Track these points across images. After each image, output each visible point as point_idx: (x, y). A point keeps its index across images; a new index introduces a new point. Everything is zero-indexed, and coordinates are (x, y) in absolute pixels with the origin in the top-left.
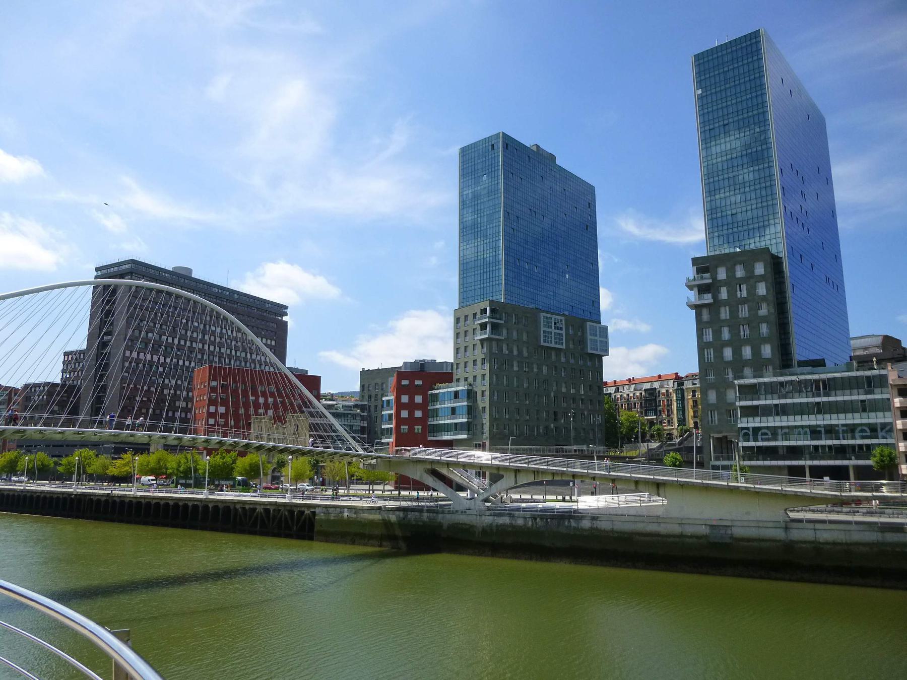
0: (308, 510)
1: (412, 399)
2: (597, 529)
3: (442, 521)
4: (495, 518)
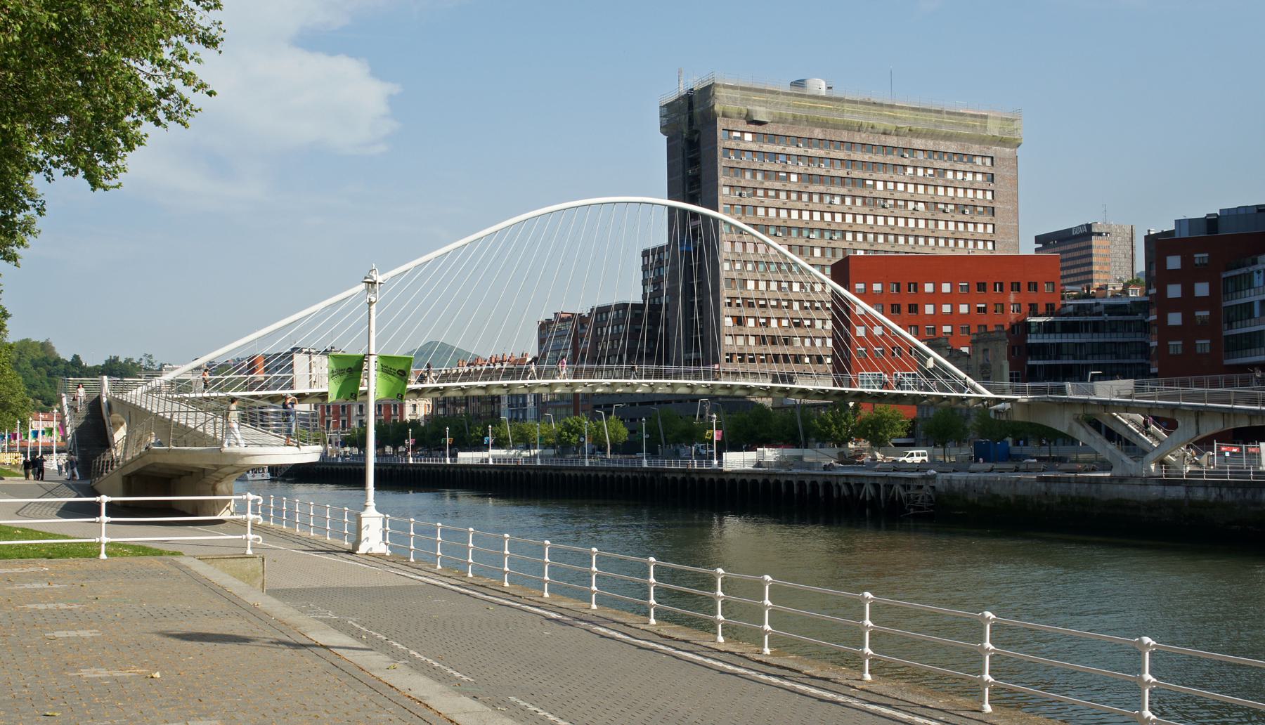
1: (1188, 290)
4: (1166, 488)
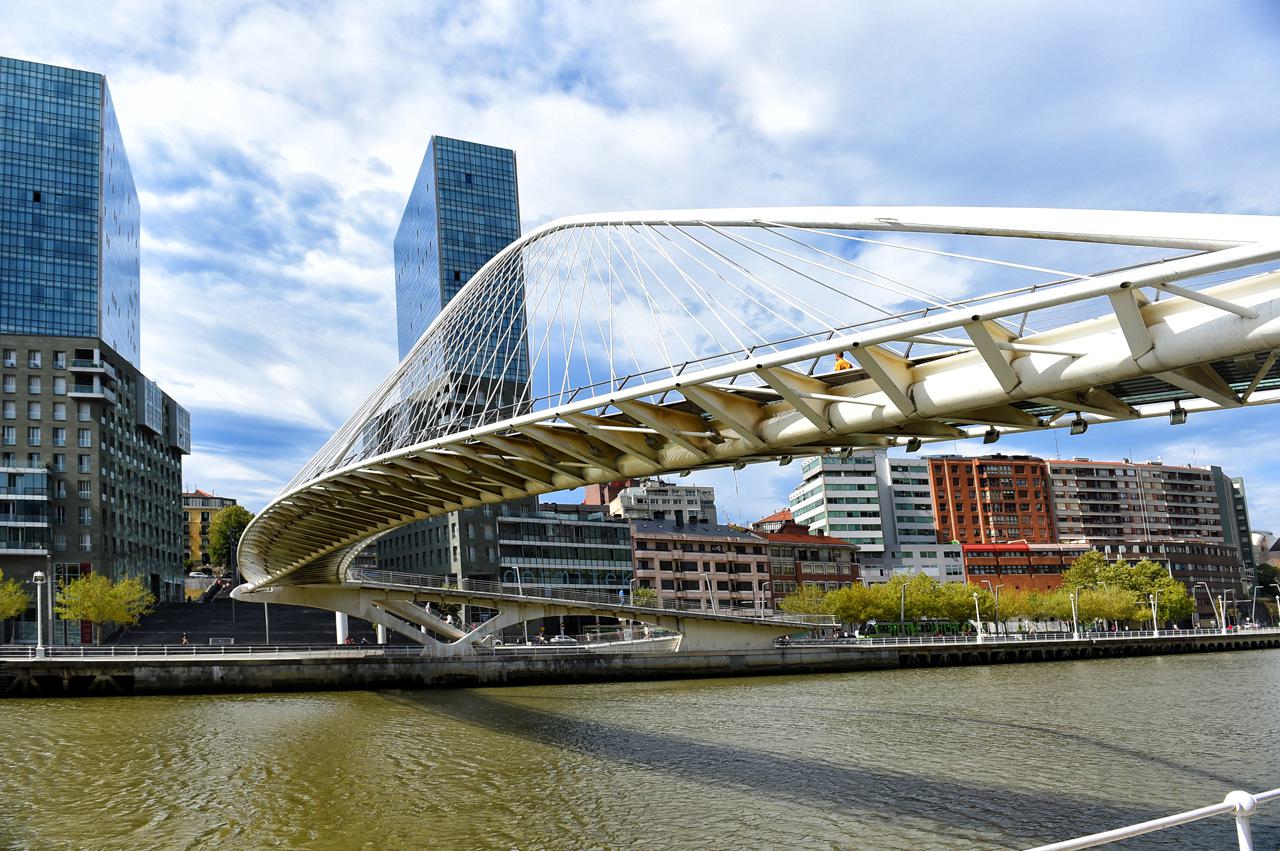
0: (103, 674)
2: (630, 667)
3: (421, 673)
